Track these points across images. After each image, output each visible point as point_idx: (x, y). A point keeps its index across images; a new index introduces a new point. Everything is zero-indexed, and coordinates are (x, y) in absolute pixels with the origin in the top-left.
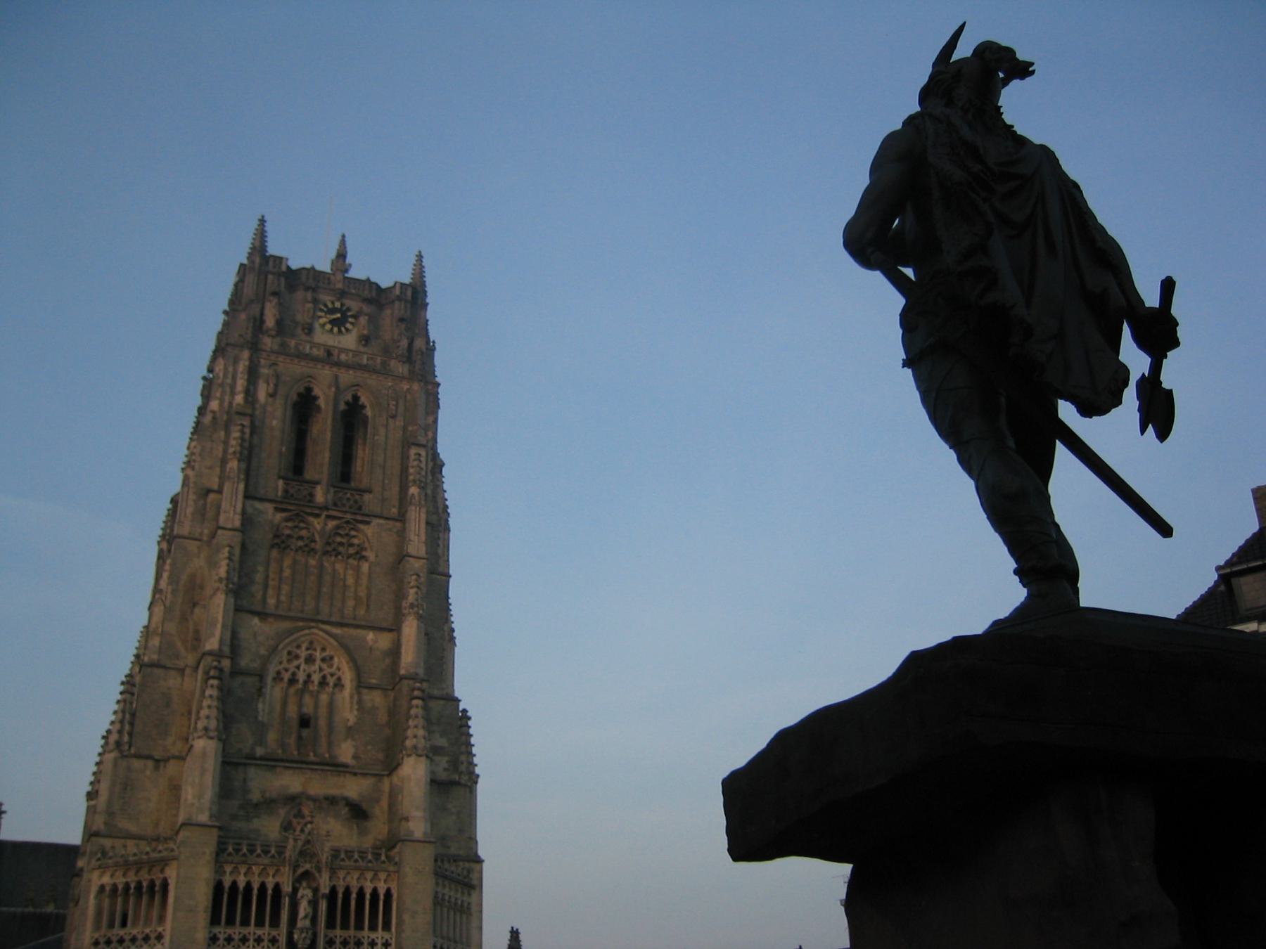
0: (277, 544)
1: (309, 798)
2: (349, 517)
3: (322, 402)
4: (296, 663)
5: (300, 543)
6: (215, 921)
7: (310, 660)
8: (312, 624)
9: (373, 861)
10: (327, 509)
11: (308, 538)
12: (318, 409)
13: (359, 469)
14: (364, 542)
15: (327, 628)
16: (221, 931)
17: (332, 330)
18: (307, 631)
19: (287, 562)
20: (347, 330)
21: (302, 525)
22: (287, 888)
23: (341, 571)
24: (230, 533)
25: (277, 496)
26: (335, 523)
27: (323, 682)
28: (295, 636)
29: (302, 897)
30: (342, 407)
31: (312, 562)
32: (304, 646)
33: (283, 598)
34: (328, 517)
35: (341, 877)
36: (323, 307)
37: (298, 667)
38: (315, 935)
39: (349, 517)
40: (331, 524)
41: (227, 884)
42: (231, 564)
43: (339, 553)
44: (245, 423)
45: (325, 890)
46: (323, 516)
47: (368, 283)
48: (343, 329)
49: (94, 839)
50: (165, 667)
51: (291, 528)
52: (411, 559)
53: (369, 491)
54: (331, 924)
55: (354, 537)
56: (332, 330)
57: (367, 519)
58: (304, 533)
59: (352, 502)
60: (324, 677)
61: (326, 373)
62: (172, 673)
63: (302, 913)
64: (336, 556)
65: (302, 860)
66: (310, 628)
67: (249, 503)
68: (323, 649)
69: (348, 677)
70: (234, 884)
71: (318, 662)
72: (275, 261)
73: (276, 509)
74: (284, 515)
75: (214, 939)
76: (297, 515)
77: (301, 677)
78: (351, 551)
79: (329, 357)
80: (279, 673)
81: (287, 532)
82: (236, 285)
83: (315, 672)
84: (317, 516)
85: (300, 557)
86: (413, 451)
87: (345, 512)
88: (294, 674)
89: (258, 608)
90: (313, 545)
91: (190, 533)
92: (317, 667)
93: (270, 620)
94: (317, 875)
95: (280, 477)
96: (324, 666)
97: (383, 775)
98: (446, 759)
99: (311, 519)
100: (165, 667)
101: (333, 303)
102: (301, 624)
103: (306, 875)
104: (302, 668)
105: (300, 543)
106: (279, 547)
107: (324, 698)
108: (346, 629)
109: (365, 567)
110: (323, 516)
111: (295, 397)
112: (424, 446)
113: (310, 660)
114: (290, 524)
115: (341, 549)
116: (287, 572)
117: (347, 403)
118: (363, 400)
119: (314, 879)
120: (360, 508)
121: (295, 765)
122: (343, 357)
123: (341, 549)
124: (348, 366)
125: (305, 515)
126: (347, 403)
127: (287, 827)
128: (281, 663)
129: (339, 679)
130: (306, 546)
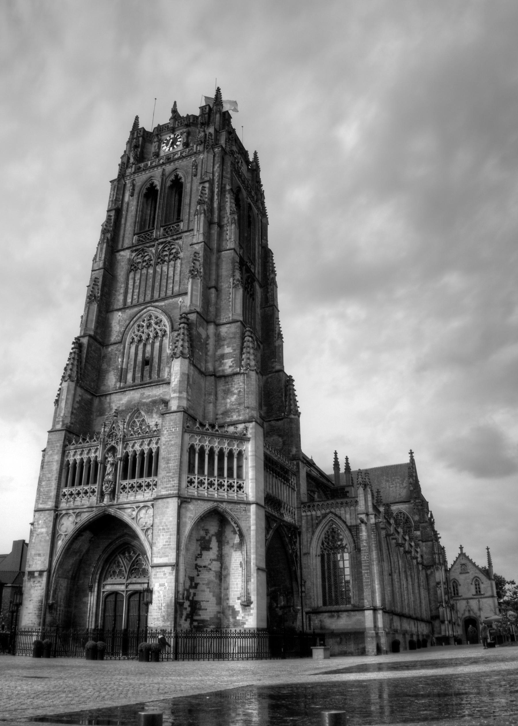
1: (144, 404)
7: (149, 326)
10: (157, 240)
14: (178, 249)
15: (157, 304)
18: (145, 310)
19: (138, 276)
20: (177, 146)
23: (166, 270)
25: (133, 243)
27: (156, 336)
28: (139, 315)
30: (169, 184)
33: (135, 297)
34: (159, 244)
40: (160, 247)
43: (165, 261)
44: (112, 215)
53: (182, 221)
55: (173, 249)
57: (179, 236)
60: (157, 333)
61: (158, 172)
65: (111, 440)
66: (146, 308)
69: (168, 329)
71: (154, 325)
73: (132, 252)
74: (136, 253)
76: (143, 250)
77: (144, 337)
78: (172, 256)
88: (141, 337)
96: (157, 327)
99: (150, 249)
102: (142, 307)
107: (157, 344)
108: (166, 302)
109: (179, 261)
111: (145, 191)
113: (149, 326)
117: (172, 181)
118: (180, 174)
121: (135, 388)
125: (147, 249)
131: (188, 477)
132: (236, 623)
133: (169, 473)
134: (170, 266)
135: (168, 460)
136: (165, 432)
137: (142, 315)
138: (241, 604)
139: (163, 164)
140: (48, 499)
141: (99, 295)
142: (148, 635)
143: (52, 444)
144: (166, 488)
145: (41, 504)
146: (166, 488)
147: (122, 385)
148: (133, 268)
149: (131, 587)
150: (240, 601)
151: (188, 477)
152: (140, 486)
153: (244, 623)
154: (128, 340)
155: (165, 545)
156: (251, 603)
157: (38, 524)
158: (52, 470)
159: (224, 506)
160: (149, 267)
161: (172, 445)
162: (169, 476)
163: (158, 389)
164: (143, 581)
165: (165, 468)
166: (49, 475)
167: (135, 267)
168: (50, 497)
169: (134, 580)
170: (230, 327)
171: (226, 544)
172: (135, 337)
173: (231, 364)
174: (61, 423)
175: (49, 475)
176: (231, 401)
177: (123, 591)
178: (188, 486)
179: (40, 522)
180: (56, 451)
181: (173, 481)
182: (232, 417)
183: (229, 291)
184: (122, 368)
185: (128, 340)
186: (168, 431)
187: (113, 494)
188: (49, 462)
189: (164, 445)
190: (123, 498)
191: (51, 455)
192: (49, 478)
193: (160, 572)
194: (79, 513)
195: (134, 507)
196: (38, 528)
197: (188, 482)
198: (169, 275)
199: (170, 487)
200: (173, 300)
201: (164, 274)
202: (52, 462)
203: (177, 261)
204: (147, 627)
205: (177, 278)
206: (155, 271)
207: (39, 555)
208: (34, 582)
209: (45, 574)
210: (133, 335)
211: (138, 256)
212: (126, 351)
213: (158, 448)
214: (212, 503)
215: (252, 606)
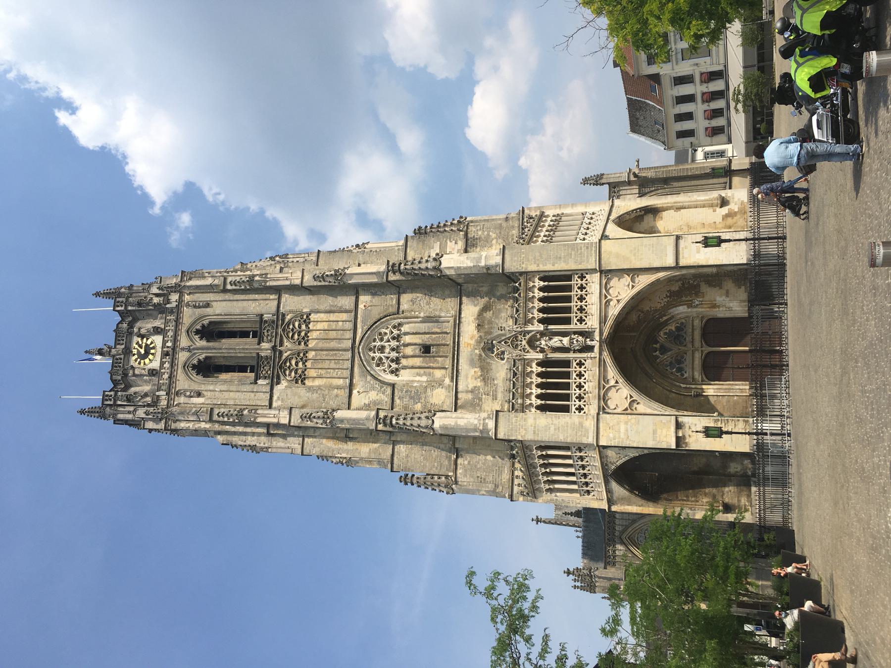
0: (302, 381)
2: (280, 330)
3: (202, 357)
4: (384, 360)
5: (300, 365)
6: (566, 409)
7: (382, 349)
8: (356, 351)
9: (518, 292)
11: (297, 359)
12: (207, 358)
13: (249, 325)
16: (574, 403)
17: (153, 354)
19: (312, 373)
20: (152, 343)
21: (288, 364)
22: (541, 356)
23: (318, 332)
24: (292, 417)
26: (285, 340)
27: (397, 338)
29: (547, 345)
30: (203, 343)
31: (311, 355)
32: (372, 354)
34: (281, 344)
35: (531, 316)
36: (137, 362)
37: (387, 358)
38: (575, 333)
39: (280, 330)
40: (287, 344)
41: (539, 402)
42: (313, 415)
45: (541, 327)
47: (117, 331)
48: (151, 346)
49: (514, 498)
50: (393, 455)
51: (291, 372)
52: (304, 280)
53: (262, 315)
54: (568, 321)
55: (294, 325)
56: (153, 354)
58: (293, 362)
59: (270, 328)
61: (182, 356)
62: (396, 450)
63: (558, 344)
64: (308, 337)
67: (275, 404)
68: (374, 340)
70: (538, 397)
71: (382, 343)
72: (107, 400)
74: (282, 378)
75: (580, 409)
76: (280, 368)
77: (394, 355)
78: (304, 327)
79: (170, 354)
80: (392, 372)
81: (293, 374)
82: (130, 425)
83: (390, 345)
84: (281, 353)
85: (309, 364)
86: (229, 287)
87: (276, 333)
89: (347, 391)
90: (302, 355)
91: (299, 444)
92: (386, 344)
93: (354, 381)
94: (530, 335)
95: (256, 383)
96: (386, 338)
97: (460, 288)
98: (448, 242)
99: (284, 358)
100: (393, 455)
101: (134, 355)
103: (532, 343)
104: (388, 355)
105: (300, 365)
106: (305, 379)
108: (358, 327)
111: (200, 377)
112: (225, 279)
114: (287, 372)
115: (303, 334)
116: (323, 372)
117: (201, 338)
119: (534, 336)
120: (273, 322)
122: (169, 344)
123: (303, 334)
124: (175, 340)
126: (201, 338)
127: (501, 356)
128: (385, 371)
130: (302, 359)
132: (741, 211)
133: (571, 254)
134: (315, 328)
135: (557, 258)
136: (524, 266)
138: (721, 207)
140: (582, 426)
142: (757, 237)
143: (512, 430)
144: (588, 257)
145: (588, 438)
146: (588, 257)
149: (697, 343)
150: (718, 209)
152: (581, 309)
154: (391, 378)
155: (653, 251)
156: (721, 195)
157: (614, 439)
158: (546, 426)
159: (614, 216)
160: (306, 357)
161: (541, 256)
162: (575, 255)
163: (464, 323)
164: (691, 327)
165: (565, 262)
166: (552, 428)
167: (300, 376)
168: (581, 424)
169: (689, 339)
170: (410, 247)
171: (654, 230)
173: (454, 242)
174: (487, 421)
175: (552, 428)
176: (496, 238)
177: (702, 351)
179: (611, 435)
180: (522, 423)
181: (581, 249)
182: (513, 235)
183: (367, 252)
185: (390, 378)
186: (523, 263)
188: (534, 433)
189: (538, 265)
191: (525, 430)
192: (555, 429)
193: (683, 253)
194: (604, 381)
196: (619, 437)
198: (326, 328)
200: (359, 316)
201: (321, 337)
202: (535, 427)
203: (312, 320)
204: (746, 264)
205: (333, 317)
207: (655, 432)
208: (689, 436)
211: (286, 375)
213: (540, 279)
214: (609, 225)
215: (723, 195)
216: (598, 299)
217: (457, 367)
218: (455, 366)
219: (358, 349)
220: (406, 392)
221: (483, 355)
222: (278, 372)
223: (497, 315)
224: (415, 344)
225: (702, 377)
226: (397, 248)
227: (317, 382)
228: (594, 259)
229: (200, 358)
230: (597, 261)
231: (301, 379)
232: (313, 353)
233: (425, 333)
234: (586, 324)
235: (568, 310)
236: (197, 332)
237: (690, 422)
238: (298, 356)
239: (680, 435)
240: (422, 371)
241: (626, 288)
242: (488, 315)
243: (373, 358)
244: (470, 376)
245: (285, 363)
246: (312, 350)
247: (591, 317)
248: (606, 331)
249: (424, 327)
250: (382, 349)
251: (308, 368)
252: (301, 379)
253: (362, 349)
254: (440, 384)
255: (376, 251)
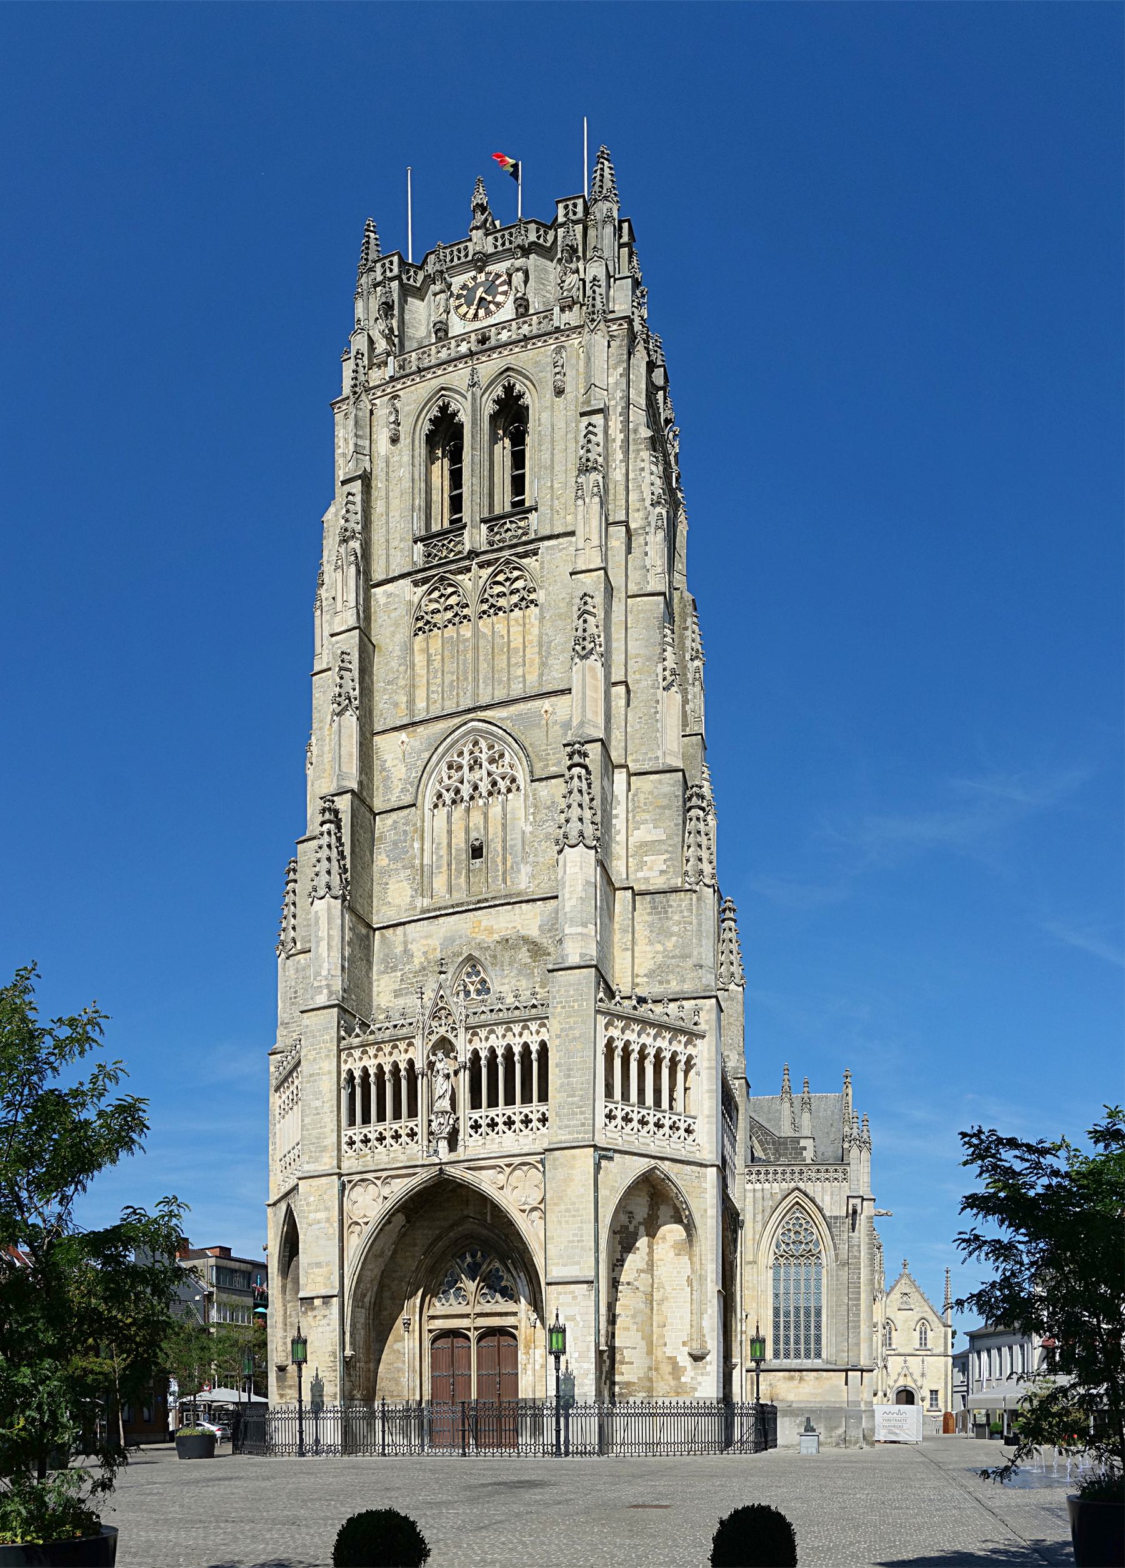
7: (475, 764)
11: (457, 605)
19: (436, 644)
25: (414, 563)
30: (489, 408)
34: (481, 566)
46: (474, 567)
54: (476, 1104)
58: (453, 600)
60: (494, 784)
61: (459, 377)
68: (491, 747)
71: (485, 764)
73: (416, 584)
76: (442, 579)
84: (468, 570)
85: (450, 631)
88: (457, 791)
90: (466, 611)
92: (484, 772)
93: (420, 729)
99: (460, 577)
105: (449, 615)
110: (474, 567)
116: (437, 664)
117: (497, 402)
129: (513, 780)
130: (456, 615)
131: (606, 1107)
137: (457, 741)
139: (471, 354)
141: (357, 692)
144: (567, 1126)
146: (567, 1126)
147: (426, 902)
148: (420, 624)
151: (606, 1107)
153: (695, 1389)
162: (572, 1104)
167: (428, 622)
170: (660, 782)
172: (444, 792)
177: (469, 1329)
178: (606, 1125)
181: (582, 1113)
183: (655, 694)
184: (422, 865)
187: (453, 1140)
190: (471, 1145)
195: (501, 1164)
197: (607, 1116)
199: (574, 1126)
206: (476, 633)
209: (335, 1300)
210: (439, 788)
211: (430, 594)
212: (426, 824)
216: (507, 1154)
217: (441, 915)
218: (443, 912)
219: (472, 720)
220: (405, 832)
221: (461, 959)
222: (434, 576)
223: (524, 971)
224: (486, 828)
225: (435, 1330)
226: (660, 753)
227: (420, 659)
228: (563, 1138)
229: (459, 414)
230: (559, 1146)
231: (423, 624)
232: (469, 634)
233: (504, 841)
234: (471, 1136)
235: (493, 1103)
236: (509, 389)
237: (331, 1317)
238: (462, 607)
239: (317, 1302)
240: (443, 851)
241: (523, 1199)
242: (524, 955)
243: (461, 754)
244: (429, 941)
245: (451, 585)
246: (476, 633)
247: (480, 1143)
248: (458, 1172)
249: (514, 838)
250: (475, 764)
251: (443, 633)
252: (423, 624)
253: (474, 730)
254: (423, 887)
255: (657, 712)
